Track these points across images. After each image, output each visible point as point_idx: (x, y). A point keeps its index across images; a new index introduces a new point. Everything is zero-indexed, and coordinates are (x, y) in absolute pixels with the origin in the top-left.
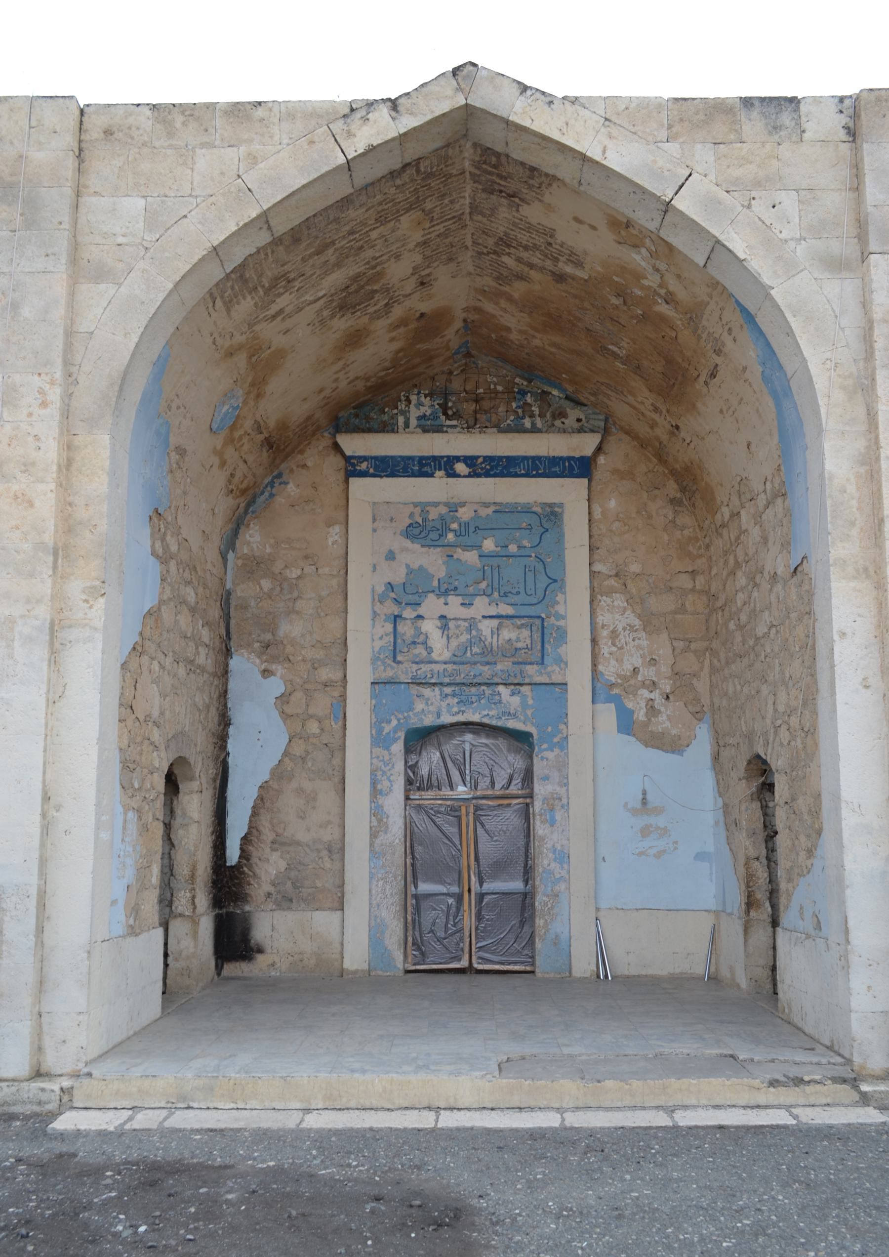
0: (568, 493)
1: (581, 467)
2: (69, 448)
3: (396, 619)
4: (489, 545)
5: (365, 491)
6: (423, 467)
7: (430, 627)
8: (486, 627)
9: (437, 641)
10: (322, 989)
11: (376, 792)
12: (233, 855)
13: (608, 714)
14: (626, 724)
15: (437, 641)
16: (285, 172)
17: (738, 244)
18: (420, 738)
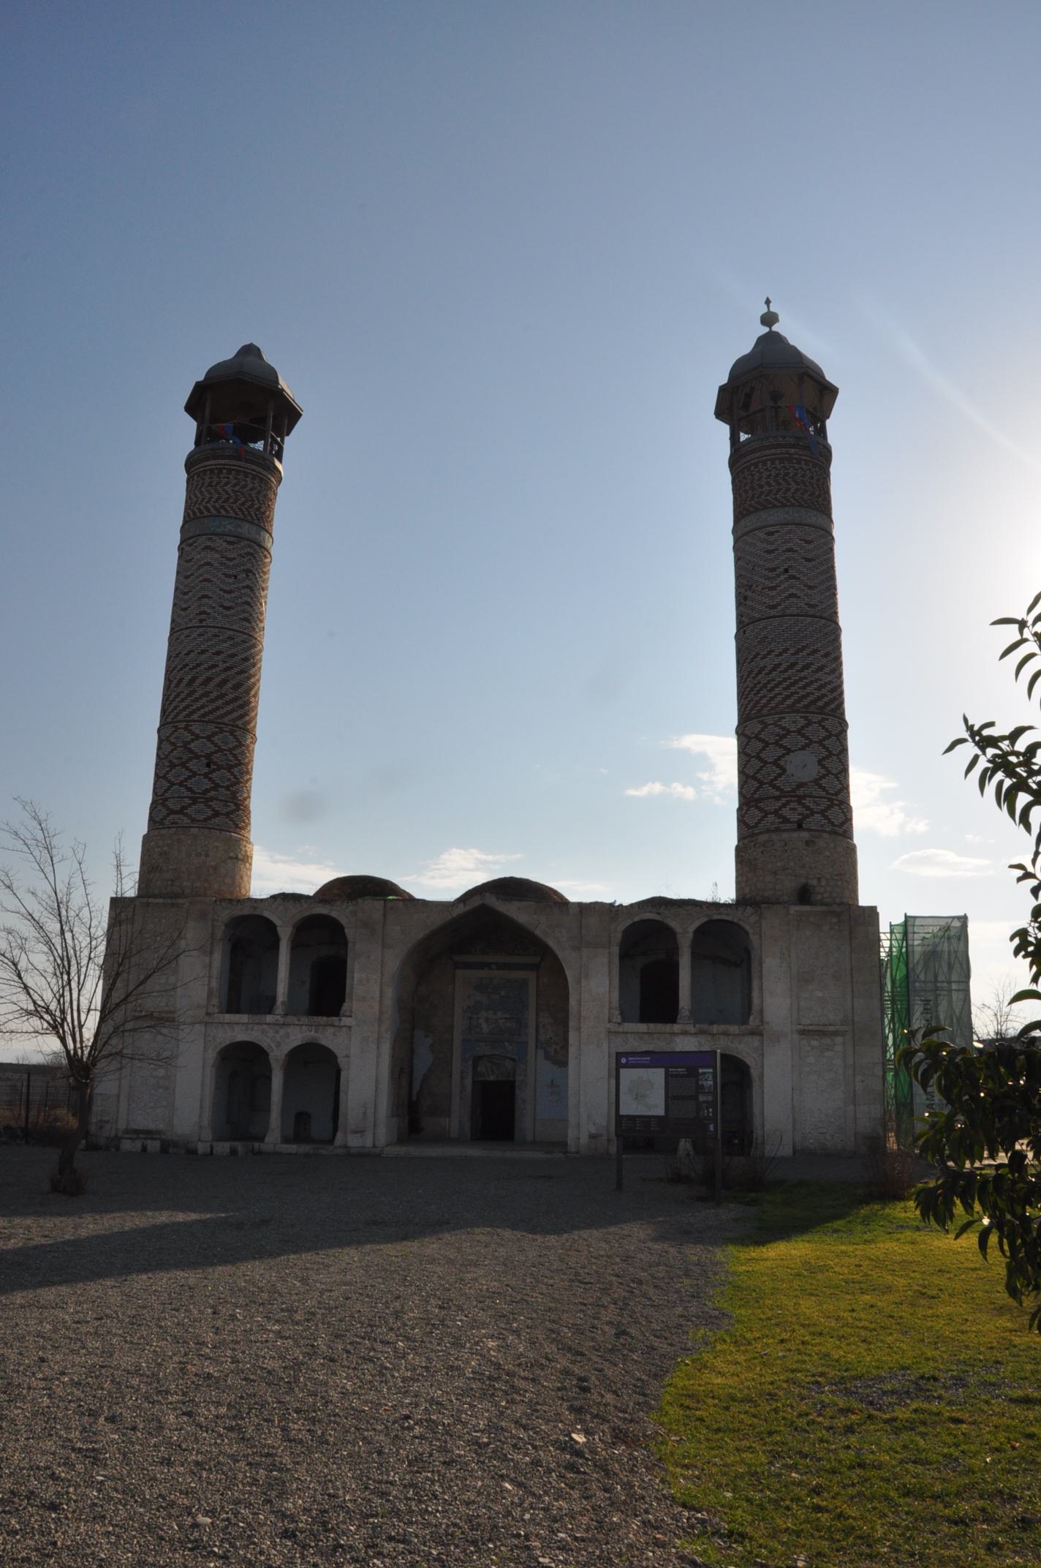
0: (531, 976)
1: (535, 967)
2: (381, 992)
3: (470, 1018)
4: (503, 993)
5: (459, 973)
6: (481, 966)
7: (481, 1021)
8: (501, 1022)
9: (484, 1026)
10: (441, 1138)
11: (462, 1078)
12: (414, 1098)
13: (541, 1053)
14: (547, 1057)
15: (484, 1026)
16: (438, 920)
17: (551, 943)
18: (477, 1060)
